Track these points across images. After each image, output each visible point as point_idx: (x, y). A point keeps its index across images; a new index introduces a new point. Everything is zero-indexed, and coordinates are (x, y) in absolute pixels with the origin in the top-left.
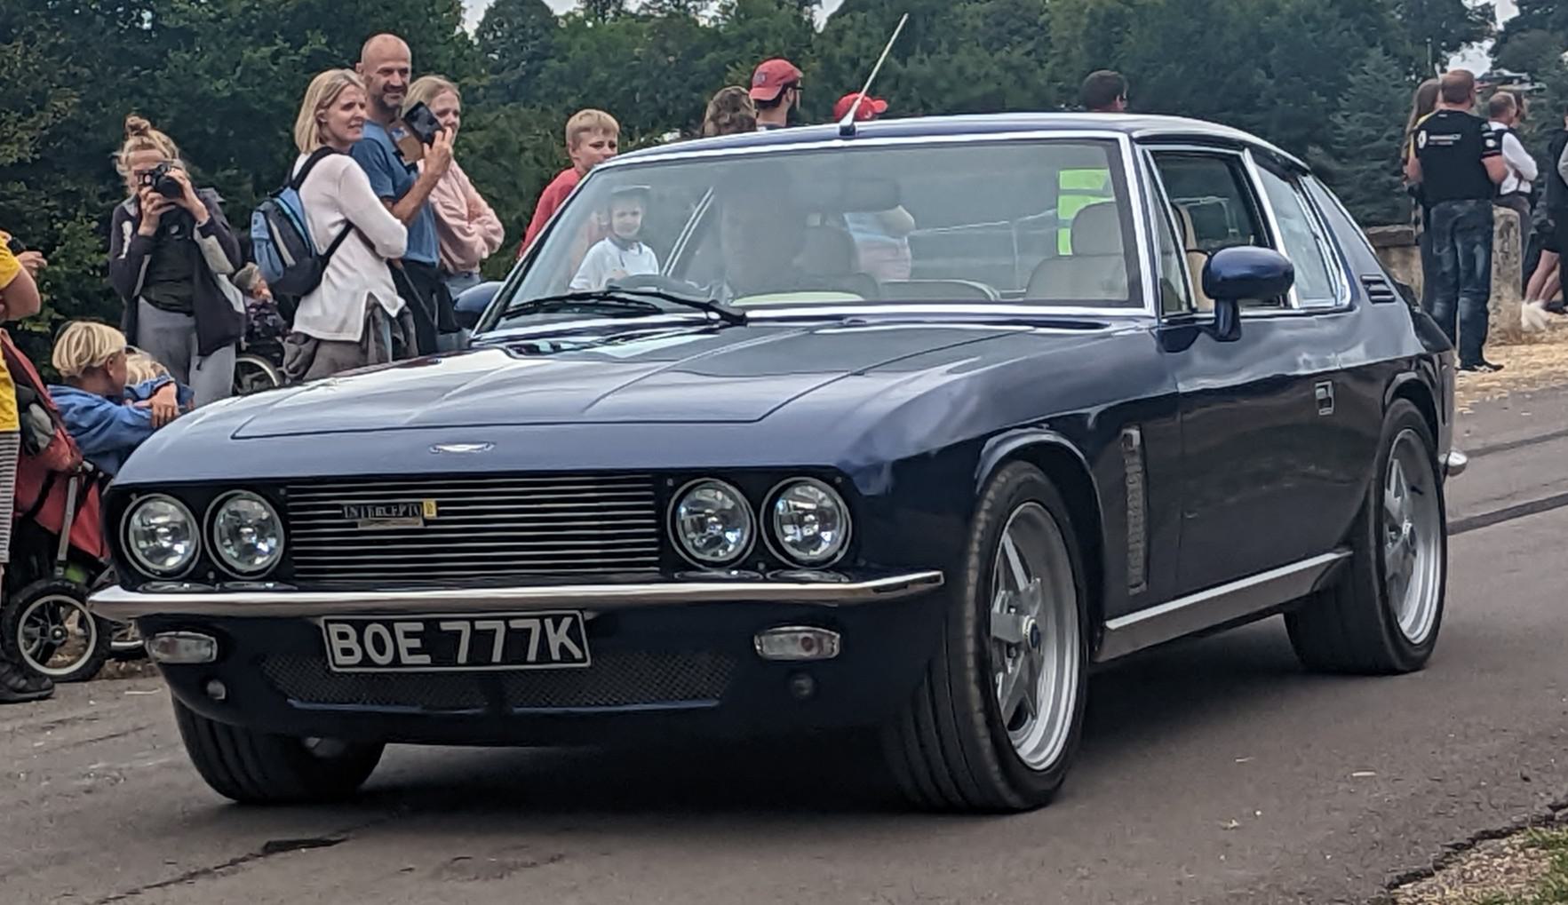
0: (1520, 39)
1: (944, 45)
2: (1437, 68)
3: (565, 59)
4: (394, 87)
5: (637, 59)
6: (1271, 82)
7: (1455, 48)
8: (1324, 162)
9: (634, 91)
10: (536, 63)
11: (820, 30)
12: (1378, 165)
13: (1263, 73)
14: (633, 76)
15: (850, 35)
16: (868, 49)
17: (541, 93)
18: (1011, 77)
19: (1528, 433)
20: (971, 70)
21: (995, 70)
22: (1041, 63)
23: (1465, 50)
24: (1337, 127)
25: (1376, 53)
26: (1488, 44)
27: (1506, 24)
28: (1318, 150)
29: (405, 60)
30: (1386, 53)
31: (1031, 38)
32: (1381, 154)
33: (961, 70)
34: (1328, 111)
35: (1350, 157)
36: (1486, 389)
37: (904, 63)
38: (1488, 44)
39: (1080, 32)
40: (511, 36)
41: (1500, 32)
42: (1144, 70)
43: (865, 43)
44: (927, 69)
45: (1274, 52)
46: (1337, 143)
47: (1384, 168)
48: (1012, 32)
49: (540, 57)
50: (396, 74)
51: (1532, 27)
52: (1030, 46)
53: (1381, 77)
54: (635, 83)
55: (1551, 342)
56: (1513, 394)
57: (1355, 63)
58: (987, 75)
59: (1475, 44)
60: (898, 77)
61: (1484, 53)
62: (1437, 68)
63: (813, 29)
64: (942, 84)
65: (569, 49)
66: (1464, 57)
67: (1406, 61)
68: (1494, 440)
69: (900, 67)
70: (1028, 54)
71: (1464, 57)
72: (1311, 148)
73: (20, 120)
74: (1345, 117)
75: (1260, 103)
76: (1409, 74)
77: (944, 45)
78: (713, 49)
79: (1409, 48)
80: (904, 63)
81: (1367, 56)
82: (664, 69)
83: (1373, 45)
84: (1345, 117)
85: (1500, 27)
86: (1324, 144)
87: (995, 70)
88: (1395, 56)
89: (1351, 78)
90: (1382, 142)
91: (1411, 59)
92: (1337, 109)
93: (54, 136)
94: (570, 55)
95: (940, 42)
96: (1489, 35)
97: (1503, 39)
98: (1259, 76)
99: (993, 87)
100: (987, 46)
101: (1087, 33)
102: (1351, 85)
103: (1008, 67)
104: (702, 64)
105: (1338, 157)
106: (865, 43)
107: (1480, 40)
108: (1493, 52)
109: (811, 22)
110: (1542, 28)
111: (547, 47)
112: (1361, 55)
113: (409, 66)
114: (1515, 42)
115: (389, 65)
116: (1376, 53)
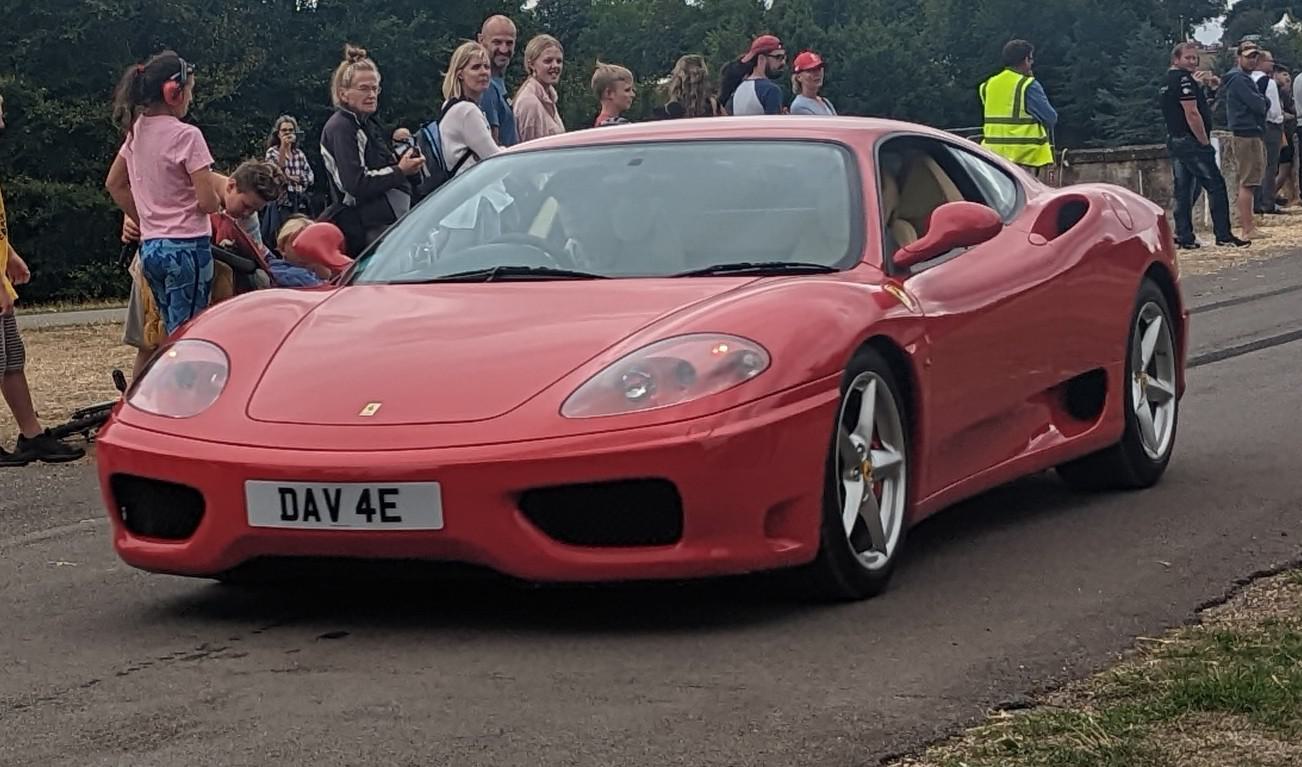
0: (1244, 16)
1: (854, 19)
2: (1187, 35)
3: (595, 27)
4: (501, 54)
5: (644, 27)
6: (1075, 45)
7: (1199, 22)
8: (1109, 100)
9: (641, 50)
10: (576, 31)
11: (768, 8)
12: (1146, 101)
13: (1068, 38)
14: (642, 38)
15: (790, 12)
16: (801, 21)
17: (579, 50)
18: (898, 40)
19: (1264, 289)
20: (870, 36)
21: (887, 36)
22: (918, 31)
23: (1207, 24)
24: (1118, 76)
25: (1146, 25)
26: (1222, 19)
27: (1234, 6)
28: (1105, 91)
29: (512, 35)
30: (1152, 25)
31: (912, 15)
32: (1148, 94)
33: (863, 36)
34: (1113, 65)
35: (1125, 96)
36: (1232, 258)
37: (827, 33)
38: (1222, 19)
39: (946, 10)
40: (559, 10)
41: (1230, 11)
42: (988, 36)
43: (800, 17)
44: (840, 36)
45: (1077, 24)
46: (1117, 86)
47: (1150, 104)
48: (899, 10)
49: (579, 25)
50: (504, 44)
51: (1252, 7)
52: (912, 20)
53: (1149, 41)
54: (643, 43)
55: (1273, 225)
56: (1251, 262)
57: (1132, 32)
58: (881, 38)
59: (1213, 19)
60: (822, 40)
61: (1219, 25)
62: (1187, 35)
63: (764, 8)
64: (851, 45)
65: (597, 21)
66: (1205, 27)
67: (1166, 32)
68: (1241, 294)
69: (823, 34)
70: (910, 25)
71: (1205, 27)
72: (1100, 90)
73: (226, 68)
74: (1124, 69)
75: (1067, 58)
76: (1168, 39)
77: (854, 19)
78: (695, 21)
79: (1168, 21)
80: (827, 33)
81: (1140, 28)
82: (662, 35)
83: (1143, 20)
84: (1124, 69)
85: (1230, 8)
86: (1108, 90)
87: (887, 36)
88: (1159, 27)
89: (1128, 42)
90: (1149, 86)
91: (1170, 29)
92: (1119, 63)
93: (249, 80)
94: (598, 24)
95: (850, 16)
96: (1222, 12)
97: (1231, 16)
98: (1065, 41)
99: (886, 47)
100: (883, 19)
101: (951, 9)
102: (1129, 48)
103: (895, 34)
104: (688, 32)
105: (1119, 95)
106: (800, 17)
107: (1217, 16)
108: (1225, 24)
109: (763, 3)
110: (1260, 8)
111: (583, 18)
112: (1137, 26)
113: (514, 39)
114: (1241, 18)
115: (499, 37)
116: (1146, 25)
